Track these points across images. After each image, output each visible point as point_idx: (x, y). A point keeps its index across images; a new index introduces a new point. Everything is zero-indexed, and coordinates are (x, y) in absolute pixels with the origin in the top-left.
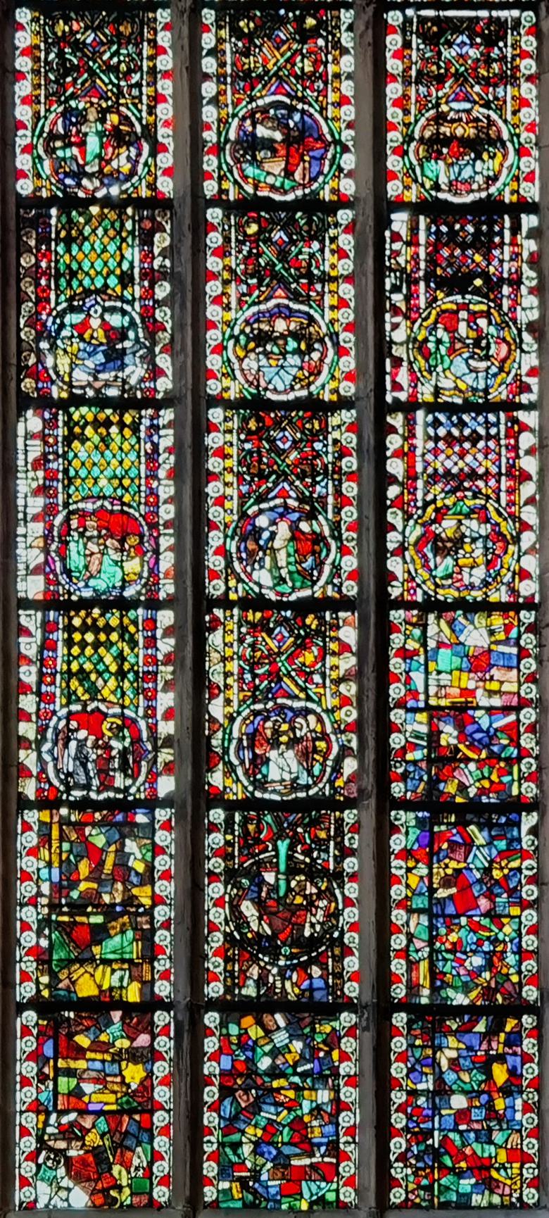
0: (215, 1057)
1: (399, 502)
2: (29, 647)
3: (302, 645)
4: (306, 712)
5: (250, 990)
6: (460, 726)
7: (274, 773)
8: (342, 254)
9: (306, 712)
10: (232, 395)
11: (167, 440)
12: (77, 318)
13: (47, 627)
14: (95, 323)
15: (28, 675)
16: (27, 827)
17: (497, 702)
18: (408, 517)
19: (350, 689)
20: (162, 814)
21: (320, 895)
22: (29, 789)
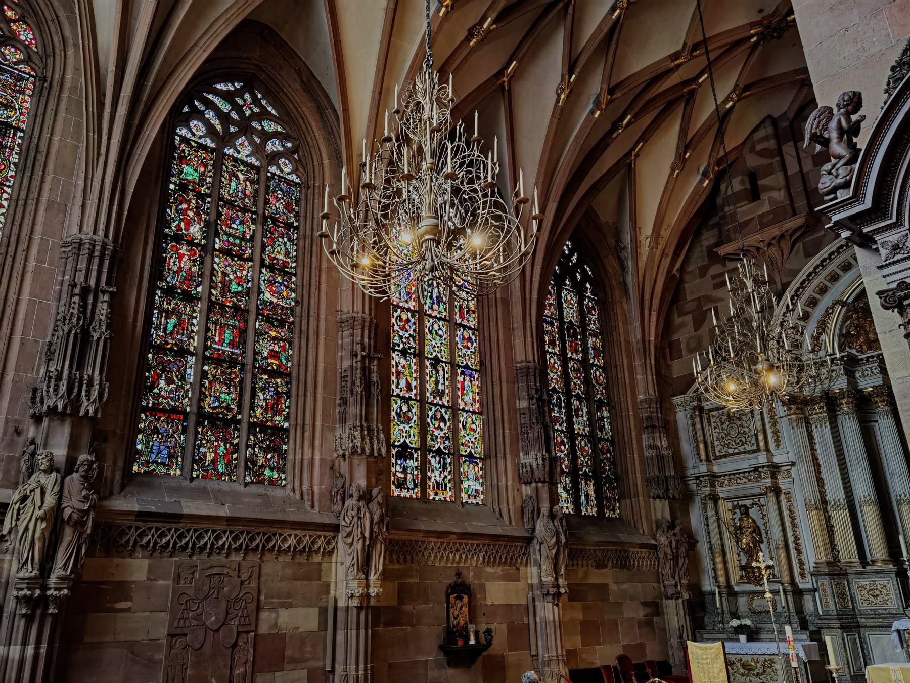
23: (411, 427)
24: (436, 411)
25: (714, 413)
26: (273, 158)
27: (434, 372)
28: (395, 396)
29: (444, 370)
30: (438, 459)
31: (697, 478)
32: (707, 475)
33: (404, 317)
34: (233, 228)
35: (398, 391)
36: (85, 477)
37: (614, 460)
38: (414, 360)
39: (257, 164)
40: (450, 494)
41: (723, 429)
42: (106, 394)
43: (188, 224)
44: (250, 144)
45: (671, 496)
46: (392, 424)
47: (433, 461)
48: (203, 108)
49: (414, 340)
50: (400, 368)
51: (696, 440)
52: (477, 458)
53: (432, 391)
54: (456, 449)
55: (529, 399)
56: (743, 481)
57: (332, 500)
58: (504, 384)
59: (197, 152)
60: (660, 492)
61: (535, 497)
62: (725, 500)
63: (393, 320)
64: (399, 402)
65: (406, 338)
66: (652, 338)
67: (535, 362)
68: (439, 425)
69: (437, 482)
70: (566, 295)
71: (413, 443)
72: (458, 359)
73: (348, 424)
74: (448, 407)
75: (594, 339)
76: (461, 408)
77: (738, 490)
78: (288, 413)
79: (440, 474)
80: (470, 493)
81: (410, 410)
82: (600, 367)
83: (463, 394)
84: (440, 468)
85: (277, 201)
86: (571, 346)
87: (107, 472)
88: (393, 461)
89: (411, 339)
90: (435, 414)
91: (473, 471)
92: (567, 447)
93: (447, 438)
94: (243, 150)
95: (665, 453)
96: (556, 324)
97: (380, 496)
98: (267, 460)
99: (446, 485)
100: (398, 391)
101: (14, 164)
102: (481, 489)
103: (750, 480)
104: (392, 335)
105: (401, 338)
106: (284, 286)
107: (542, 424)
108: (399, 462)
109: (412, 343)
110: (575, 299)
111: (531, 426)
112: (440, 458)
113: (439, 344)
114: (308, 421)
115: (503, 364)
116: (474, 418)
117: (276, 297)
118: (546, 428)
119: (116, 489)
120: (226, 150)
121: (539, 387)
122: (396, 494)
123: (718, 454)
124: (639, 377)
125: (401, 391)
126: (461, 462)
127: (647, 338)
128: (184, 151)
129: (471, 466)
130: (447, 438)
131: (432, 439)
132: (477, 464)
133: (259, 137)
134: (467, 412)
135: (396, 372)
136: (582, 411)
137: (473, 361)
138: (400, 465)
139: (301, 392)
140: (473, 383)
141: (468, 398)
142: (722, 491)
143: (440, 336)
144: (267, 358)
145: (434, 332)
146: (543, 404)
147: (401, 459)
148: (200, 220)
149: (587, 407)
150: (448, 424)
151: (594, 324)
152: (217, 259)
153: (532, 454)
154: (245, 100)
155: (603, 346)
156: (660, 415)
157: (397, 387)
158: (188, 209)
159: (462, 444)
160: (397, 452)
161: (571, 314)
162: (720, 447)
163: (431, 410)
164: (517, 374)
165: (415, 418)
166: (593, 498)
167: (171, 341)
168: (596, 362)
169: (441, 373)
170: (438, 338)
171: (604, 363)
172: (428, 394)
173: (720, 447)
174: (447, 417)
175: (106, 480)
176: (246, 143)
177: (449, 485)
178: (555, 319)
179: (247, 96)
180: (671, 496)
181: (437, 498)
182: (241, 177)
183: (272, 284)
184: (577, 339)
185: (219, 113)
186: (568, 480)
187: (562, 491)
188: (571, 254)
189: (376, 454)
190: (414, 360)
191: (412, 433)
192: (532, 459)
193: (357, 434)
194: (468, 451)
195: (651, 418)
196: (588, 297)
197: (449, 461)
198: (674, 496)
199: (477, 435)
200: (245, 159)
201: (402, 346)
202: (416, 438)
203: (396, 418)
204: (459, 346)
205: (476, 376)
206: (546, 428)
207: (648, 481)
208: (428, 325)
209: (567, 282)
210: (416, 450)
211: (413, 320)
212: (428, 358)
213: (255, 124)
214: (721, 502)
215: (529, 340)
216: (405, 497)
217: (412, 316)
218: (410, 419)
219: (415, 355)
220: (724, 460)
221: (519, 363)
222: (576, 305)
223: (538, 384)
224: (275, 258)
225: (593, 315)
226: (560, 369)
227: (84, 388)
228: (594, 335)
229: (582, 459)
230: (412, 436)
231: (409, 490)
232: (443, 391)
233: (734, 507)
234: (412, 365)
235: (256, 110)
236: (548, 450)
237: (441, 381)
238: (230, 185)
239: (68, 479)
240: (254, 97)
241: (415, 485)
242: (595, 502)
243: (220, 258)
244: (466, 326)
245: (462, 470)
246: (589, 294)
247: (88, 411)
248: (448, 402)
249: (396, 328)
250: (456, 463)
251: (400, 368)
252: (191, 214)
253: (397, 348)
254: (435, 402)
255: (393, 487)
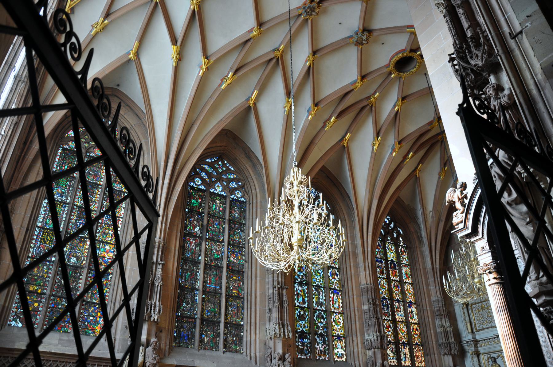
0: (51, 304)
1: (100, 226)
2: (36, 233)
3: (80, 243)
4: (79, 253)
5: (60, 294)
6: (103, 260)
7: (72, 261)
8: (99, 191)
9: (79, 253)
10: (78, 205)
11: (66, 209)
12: (57, 189)
13: (40, 231)
14: (60, 190)
15: (35, 237)
16: (28, 261)
17: (109, 257)
18: (101, 228)
19: (87, 251)
20: (51, 263)
21: (75, 281)
22: (30, 255)
23: (305, 322)
25: (474, 306)
26: (232, 191)
30: (320, 338)
31: (467, 342)
32: (472, 341)
34: (215, 227)
36: (154, 349)
37: (420, 335)
39: (225, 195)
41: (480, 314)
42: (161, 311)
43: (194, 227)
44: (221, 186)
45: (453, 353)
47: (318, 340)
48: (200, 172)
51: (466, 322)
52: (342, 337)
55: (369, 305)
56: (492, 343)
57: (265, 360)
58: (355, 297)
59: (198, 192)
60: (447, 352)
61: (373, 357)
62: (483, 354)
64: (299, 309)
66: (438, 266)
67: (371, 284)
69: (320, 350)
70: (388, 246)
73: (272, 322)
75: (406, 268)
76: (332, 311)
77: (489, 348)
78: (243, 317)
79: (322, 346)
81: (305, 313)
82: (410, 283)
83: (333, 303)
85: (235, 212)
86: (393, 273)
87: (163, 346)
91: (340, 344)
92: (392, 328)
94: (218, 189)
95: (448, 329)
96: (383, 262)
97: (289, 358)
98: (233, 340)
99: (325, 352)
100: (298, 303)
101: (124, 208)
102: (345, 353)
103: (495, 343)
105: (299, 276)
106: (239, 253)
107: (376, 318)
109: (305, 278)
110: (393, 247)
111: (370, 319)
113: (319, 278)
114: (253, 321)
115: (354, 287)
117: (236, 260)
118: (378, 319)
119: (167, 355)
120: (211, 190)
121: (374, 298)
122: (299, 357)
123: (478, 328)
124: (432, 288)
127: (435, 266)
128: (192, 193)
129: (339, 341)
132: (342, 340)
133: (226, 182)
134: (335, 313)
136: (400, 308)
137: (338, 286)
139: (249, 306)
141: (336, 306)
142: (481, 350)
143: (320, 273)
144: (232, 290)
146: (376, 307)
148: (199, 225)
149: (403, 306)
151: (405, 260)
152: (207, 243)
153: (371, 334)
154: (219, 165)
155: (411, 272)
156: (444, 308)
157: (297, 302)
158: (194, 220)
161: (391, 256)
162: (479, 324)
164: (362, 292)
166: (408, 356)
167: (188, 284)
168: (407, 281)
169: (321, 293)
170: (318, 274)
171: (412, 281)
173: (479, 324)
175: (162, 351)
176: (220, 185)
178: (383, 259)
179: (220, 163)
180: (453, 353)
181: (321, 359)
182: (218, 202)
183: (234, 253)
184: (396, 269)
185: (207, 173)
186: (393, 347)
187: (390, 353)
188: (390, 223)
189: (286, 337)
192: (371, 336)
193: (277, 327)
194: (337, 333)
195: (440, 310)
196: (401, 246)
198: (455, 353)
200: (220, 193)
201: (299, 280)
206: (378, 319)
207: (439, 346)
209: (389, 238)
213: (224, 176)
214: (481, 356)
215: (367, 272)
216: (304, 358)
218: (305, 318)
220: (481, 332)
221: (363, 285)
222: (394, 250)
223: (373, 296)
224: (234, 240)
225: (404, 255)
226: (387, 286)
227: (153, 308)
228: (405, 266)
229: (401, 335)
232: (322, 303)
233: (489, 358)
234: (305, 289)
235: (224, 169)
236: (380, 332)
237: (321, 297)
238: (213, 206)
239: (147, 349)
240: (223, 163)
242: (410, 358)
243: (209, 242)
244: (334, 267)
245: (334, 343)
246: (402, 244)
247: (154, 319)
251: (298, 291)
252: (195, 222)
254: (318, 308)
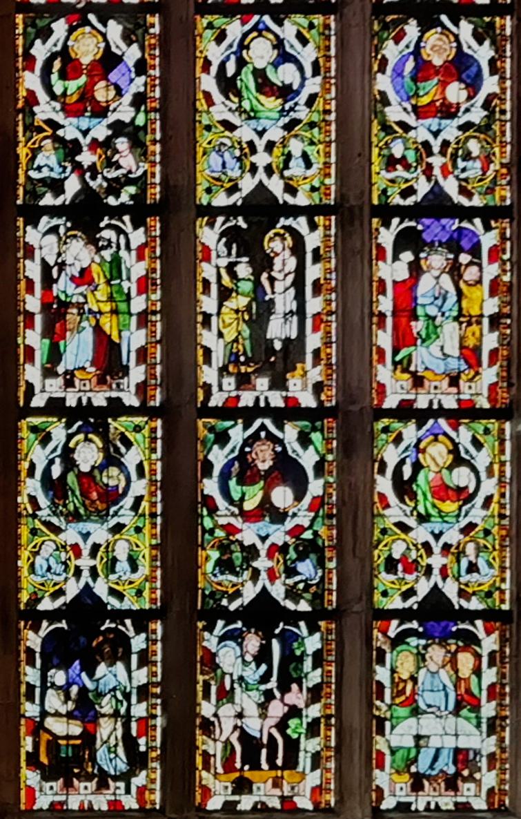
24: (249, 442)
27: (244, 270)
28: (38, 412)
29: (298, 248)
30: (253, 643)
33: (86, 49)
35: (55, 387)
38: (137, 238)
40: (314, 779)
46: (24, 532)
47: (228, 657)
49: (138, 144)
50: (64, 287)
53: (233, 358)
54: (355, 588)
63: (31, 81)
65: (95, 144)
68: (266, 499)
69: (245, 737)
71: (129, 592)
72: (381, 178)
74: (314, 416)
79: (263, 707)
80: (423, 765)
84: (265, 678)
88: (31, 675)
89: (122, 144)
90: (242, 457)
93: (310, 549)
99: (292, 747)
104: (23, 151)
105: (70, 149)
108: (59, 677)
112: (267, 636)
113: (275, 134)
116: (464, 436)
125: (69, 383)
126: (379, 639)
130: (310, 549)
131: (225, 565)
135: (46, 307)
138: (65, 690)
140: (471, 274)
143: (286, 92)
145: (247, 79)
147: (65, 665)
150: (315, 487)
159: (391, 565)
160: (45, 641)
163: (222, 438)
165: (139, 487)
169: (285, 263)
172: (209, 375)
174: (308, 459)
177: (310, 746)
181: (246, 803)
190: (137, 238)
191: (121, 551)
197: (313, 643)
199: (477, 514)
202: (144, 569)
203: (43, 501)
204: (394, 113)
205: (489, 240)
208: (215, 53)
210: (141, 620)
211: (132, 54)
212: (211, 213)
217: (127, 38)
219: (139, 212)
230: (123, 566)
231: (103, 781)
234: (128, 259)
237: (284, 301)
241: (137, 761)
245: (382, 674)
248: (318, 388)
249: (45, 110)
250: (354, 647)
251: (64, 287)
253: (48, 200)
254: (247, 399)
255: (30, 777)
